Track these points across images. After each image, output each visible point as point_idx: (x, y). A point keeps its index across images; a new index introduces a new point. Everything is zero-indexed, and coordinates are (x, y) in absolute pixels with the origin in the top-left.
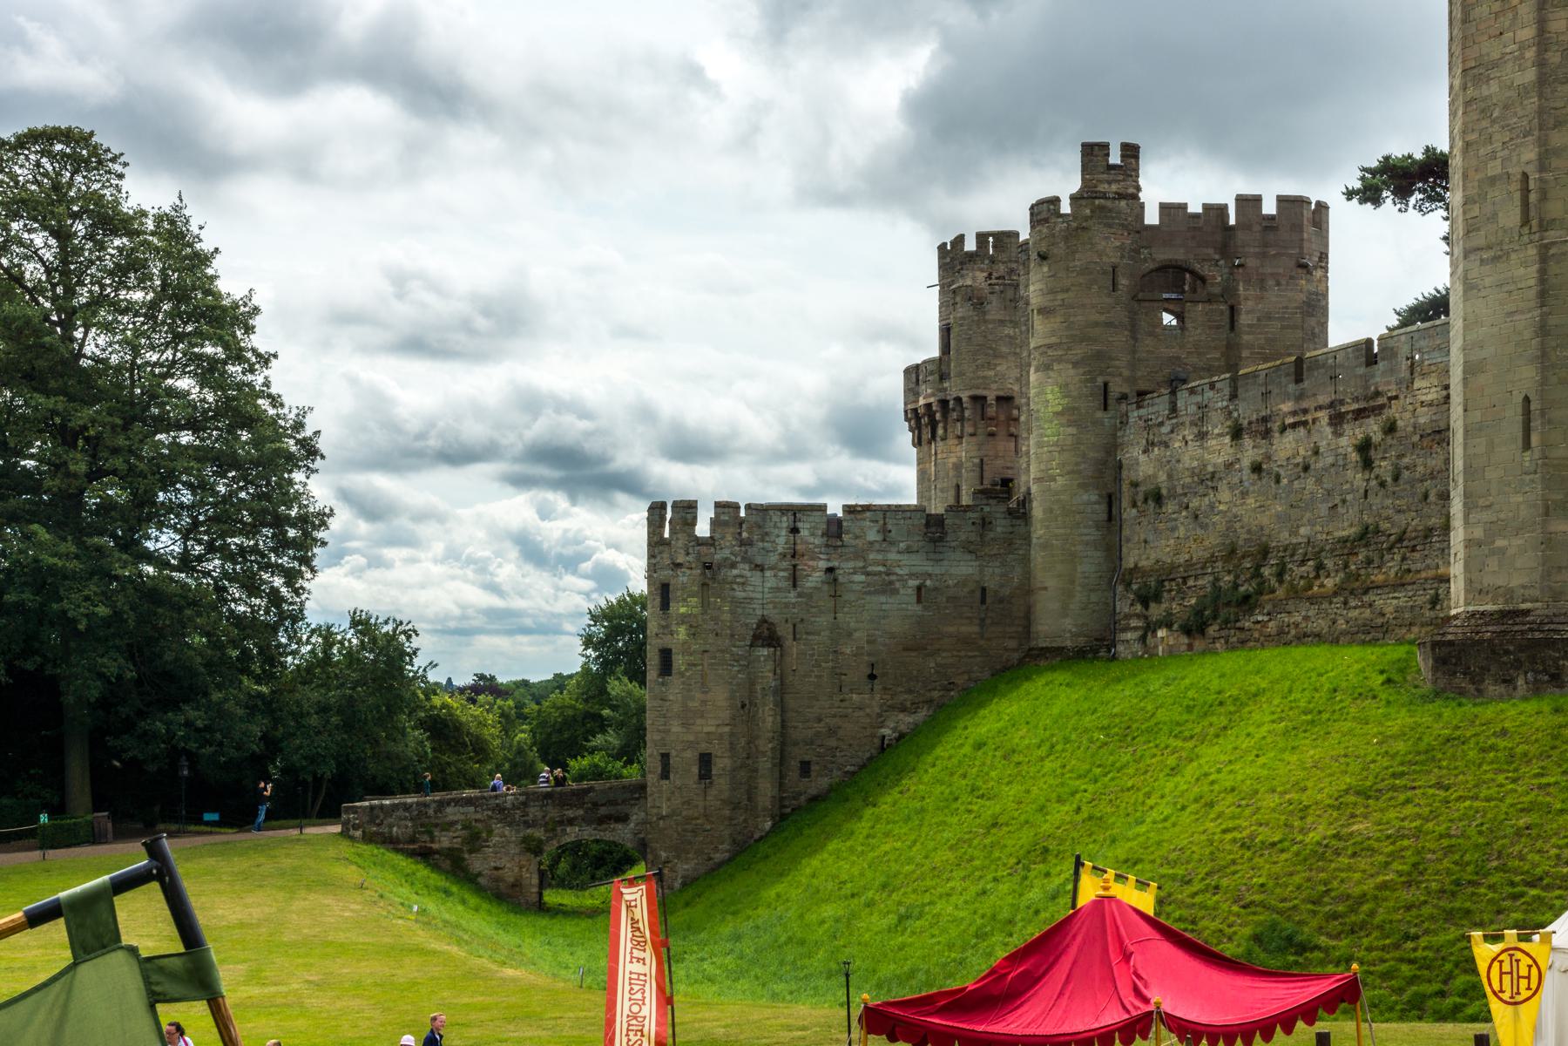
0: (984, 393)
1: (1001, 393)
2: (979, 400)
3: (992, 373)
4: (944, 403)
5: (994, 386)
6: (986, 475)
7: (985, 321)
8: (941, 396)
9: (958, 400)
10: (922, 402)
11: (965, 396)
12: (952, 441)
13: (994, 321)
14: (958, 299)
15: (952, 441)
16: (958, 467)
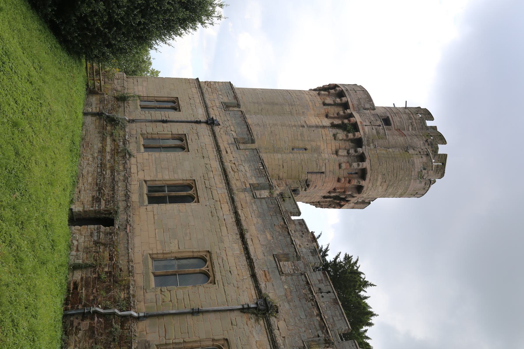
0: (367, 179)
1: (365, 189)
2: (363, 174)
3: (379, 183)
4: (358, 143)
5: (370, 185)
6: (314, 176)
7: (410, 180)
8: (365, 142)
9: (362, 158)
10: (357, 118)
11: (366, 165)
12: (335, 145)
13: (409, 185)
14: (425, 159)
15: (335, 145)
16: (317, 150)
